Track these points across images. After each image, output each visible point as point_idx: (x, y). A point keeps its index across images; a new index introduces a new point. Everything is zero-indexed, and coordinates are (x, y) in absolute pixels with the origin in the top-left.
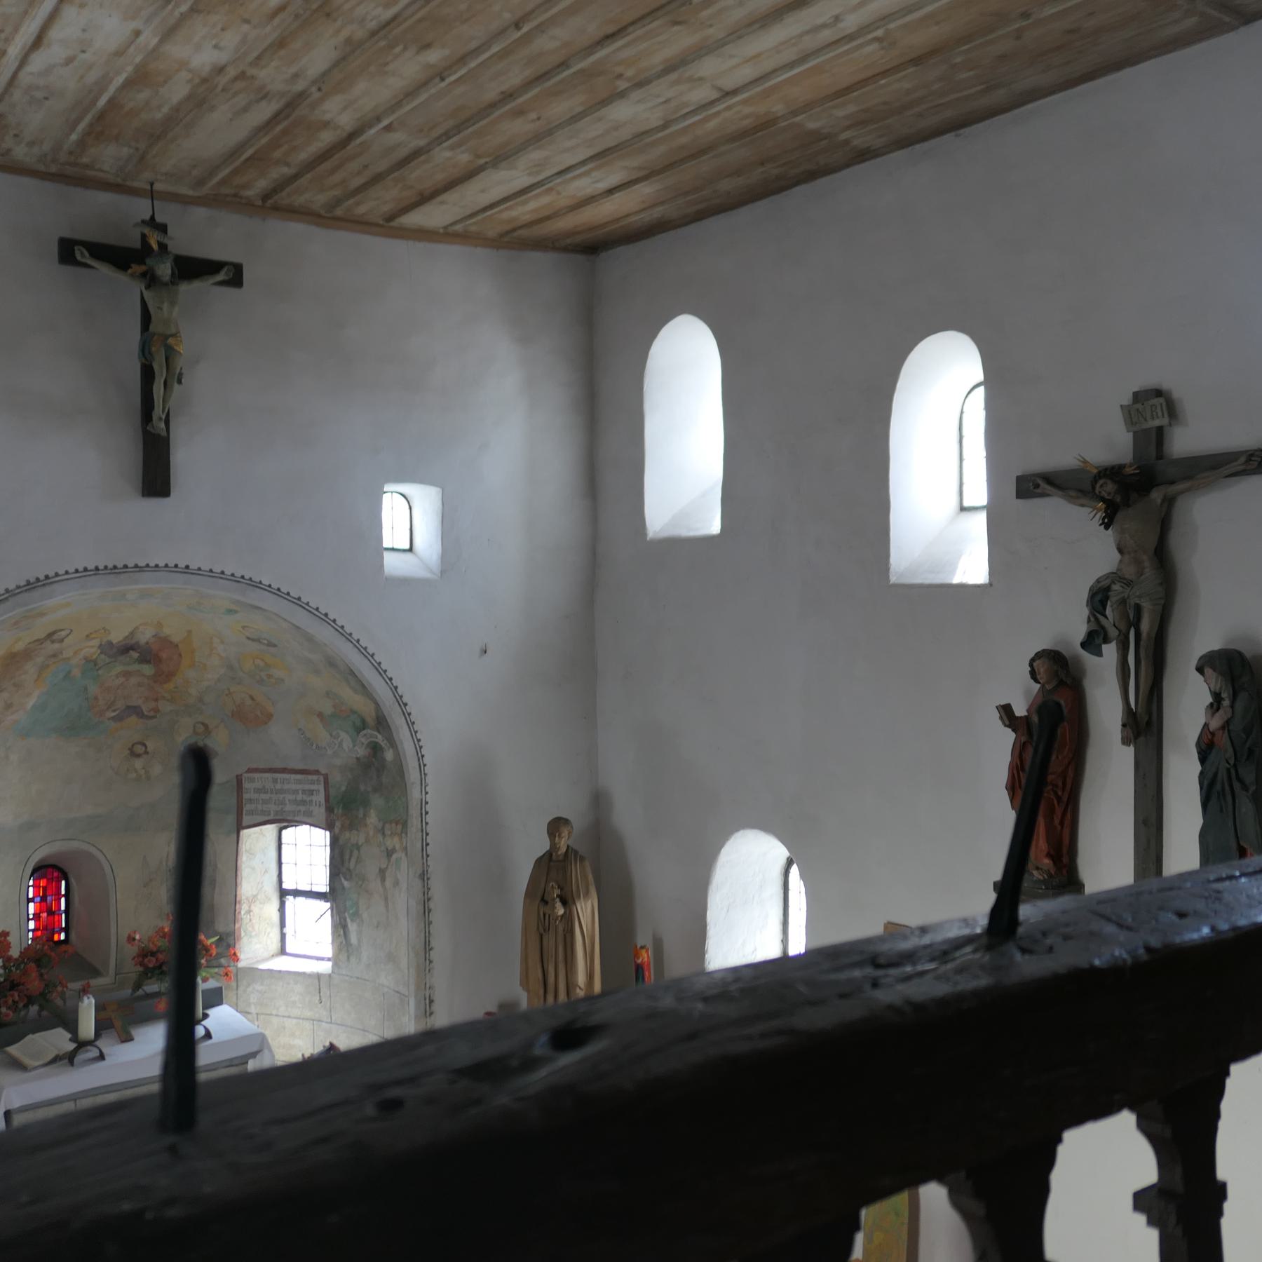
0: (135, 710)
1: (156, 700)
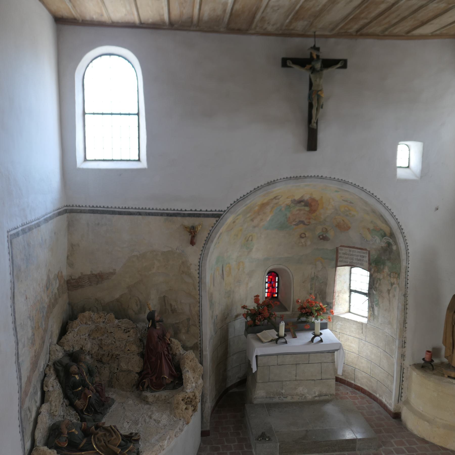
0: (302, 222)
1: (310, 219)
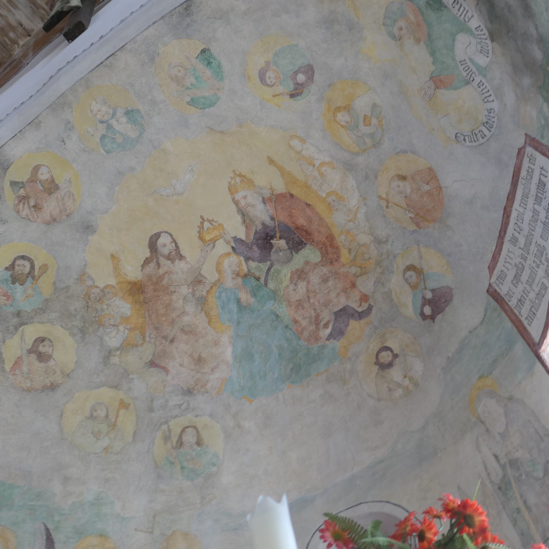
0: (344, 314)
1: (354, 285)
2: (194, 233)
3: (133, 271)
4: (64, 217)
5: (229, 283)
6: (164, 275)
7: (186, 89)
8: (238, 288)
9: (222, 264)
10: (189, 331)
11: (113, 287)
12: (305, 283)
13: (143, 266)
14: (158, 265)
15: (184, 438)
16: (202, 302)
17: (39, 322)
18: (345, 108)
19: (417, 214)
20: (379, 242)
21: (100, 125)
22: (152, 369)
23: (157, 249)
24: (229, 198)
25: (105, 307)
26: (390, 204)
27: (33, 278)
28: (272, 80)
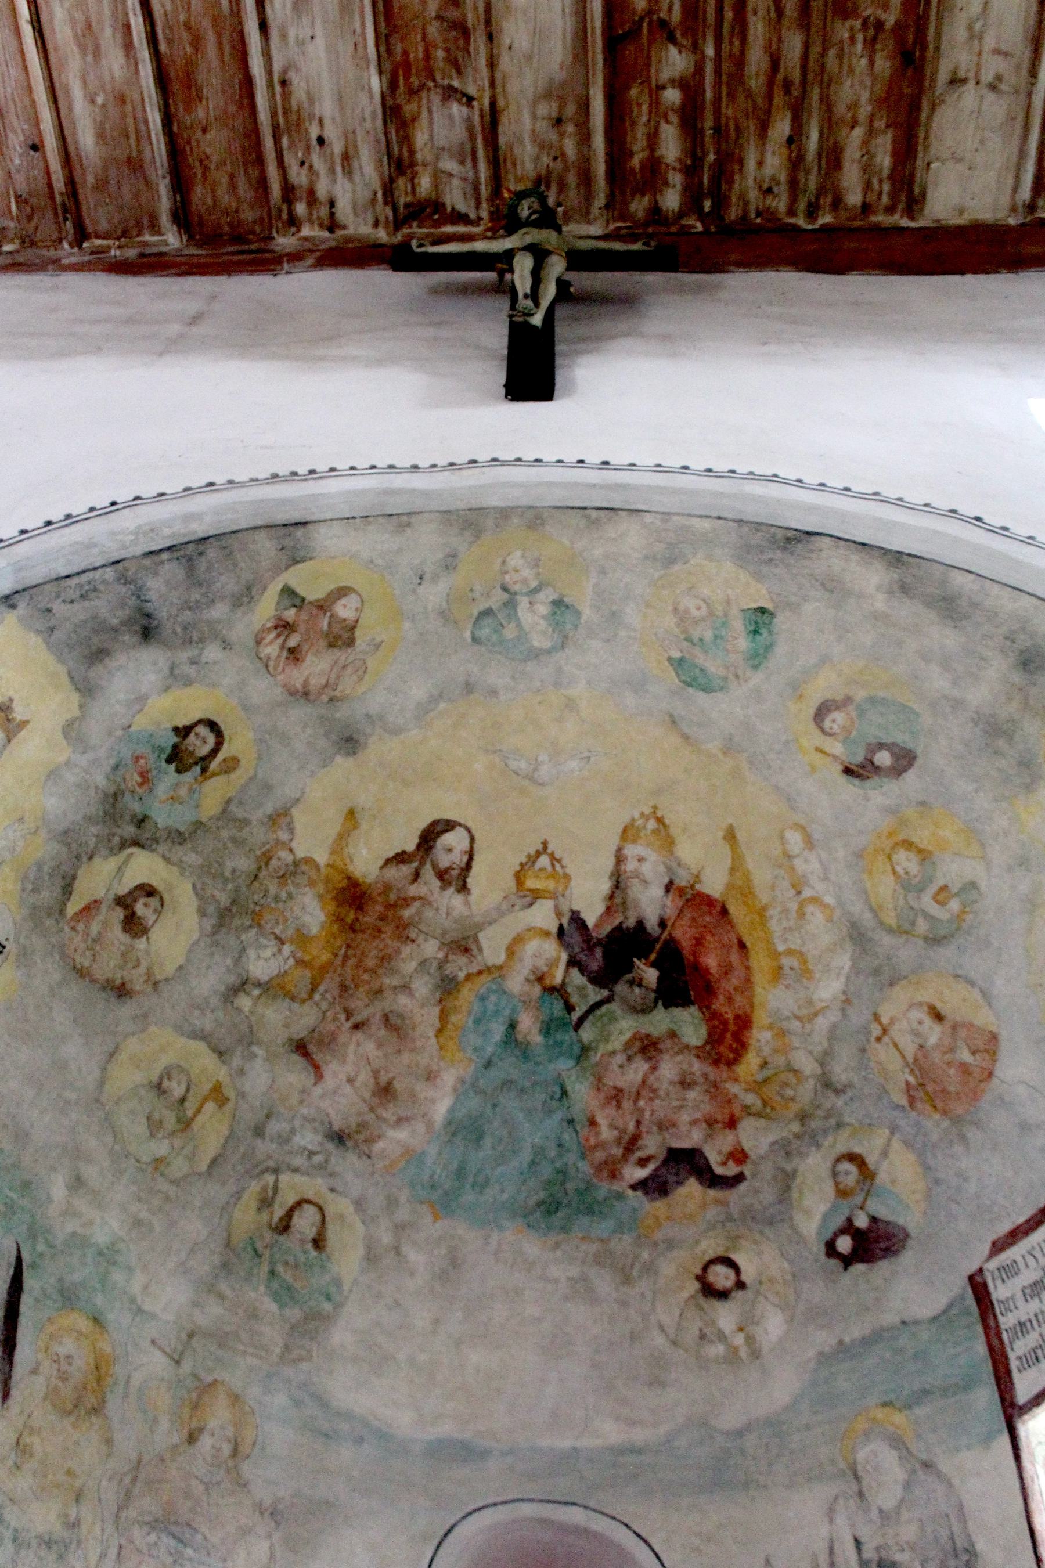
0: (686, 1162)
1: (732, 1123)
2: (515, 860)
3: (366, 862)
4: (325, 698)
5: (516, 982)
6: (414, 899)
7: (686, 639)
8: (524, 1002)
9: (524, 944)
10: (395, 1026)
11: (317, 867)
12: (646, 1066)
13: (388, 862)
14: (417, 876)
15: (296, 1220)
16: (448, 987)
17: (164, 857)
18: (920, 851)
19: (922, 1085)
20: (827, 1084)
21: (499, 591)
22: (296, 1057)
23: (431, 848)
24: (614, 841)
25: (284, 895)
26: (886, 1039)
27: (204, 770)
28: (835, 726)
